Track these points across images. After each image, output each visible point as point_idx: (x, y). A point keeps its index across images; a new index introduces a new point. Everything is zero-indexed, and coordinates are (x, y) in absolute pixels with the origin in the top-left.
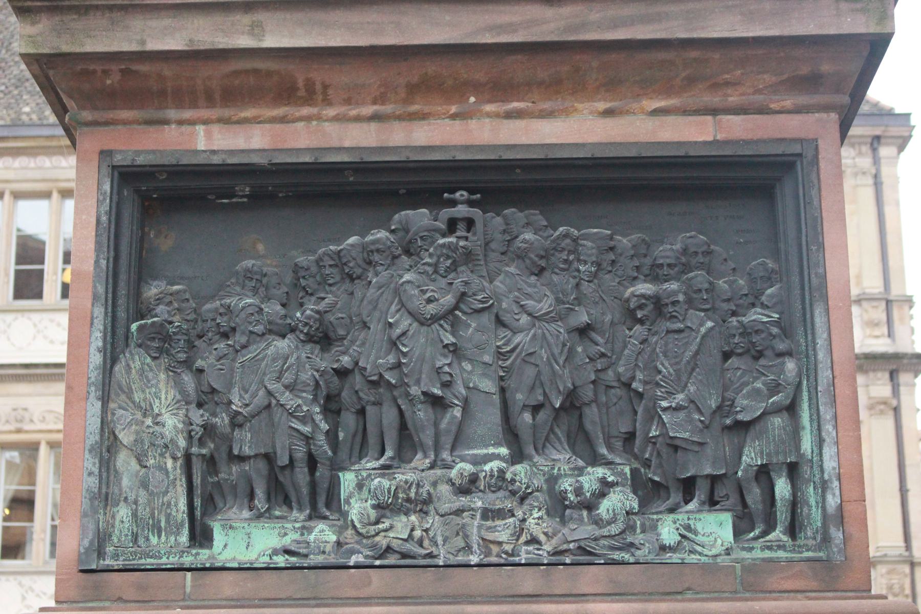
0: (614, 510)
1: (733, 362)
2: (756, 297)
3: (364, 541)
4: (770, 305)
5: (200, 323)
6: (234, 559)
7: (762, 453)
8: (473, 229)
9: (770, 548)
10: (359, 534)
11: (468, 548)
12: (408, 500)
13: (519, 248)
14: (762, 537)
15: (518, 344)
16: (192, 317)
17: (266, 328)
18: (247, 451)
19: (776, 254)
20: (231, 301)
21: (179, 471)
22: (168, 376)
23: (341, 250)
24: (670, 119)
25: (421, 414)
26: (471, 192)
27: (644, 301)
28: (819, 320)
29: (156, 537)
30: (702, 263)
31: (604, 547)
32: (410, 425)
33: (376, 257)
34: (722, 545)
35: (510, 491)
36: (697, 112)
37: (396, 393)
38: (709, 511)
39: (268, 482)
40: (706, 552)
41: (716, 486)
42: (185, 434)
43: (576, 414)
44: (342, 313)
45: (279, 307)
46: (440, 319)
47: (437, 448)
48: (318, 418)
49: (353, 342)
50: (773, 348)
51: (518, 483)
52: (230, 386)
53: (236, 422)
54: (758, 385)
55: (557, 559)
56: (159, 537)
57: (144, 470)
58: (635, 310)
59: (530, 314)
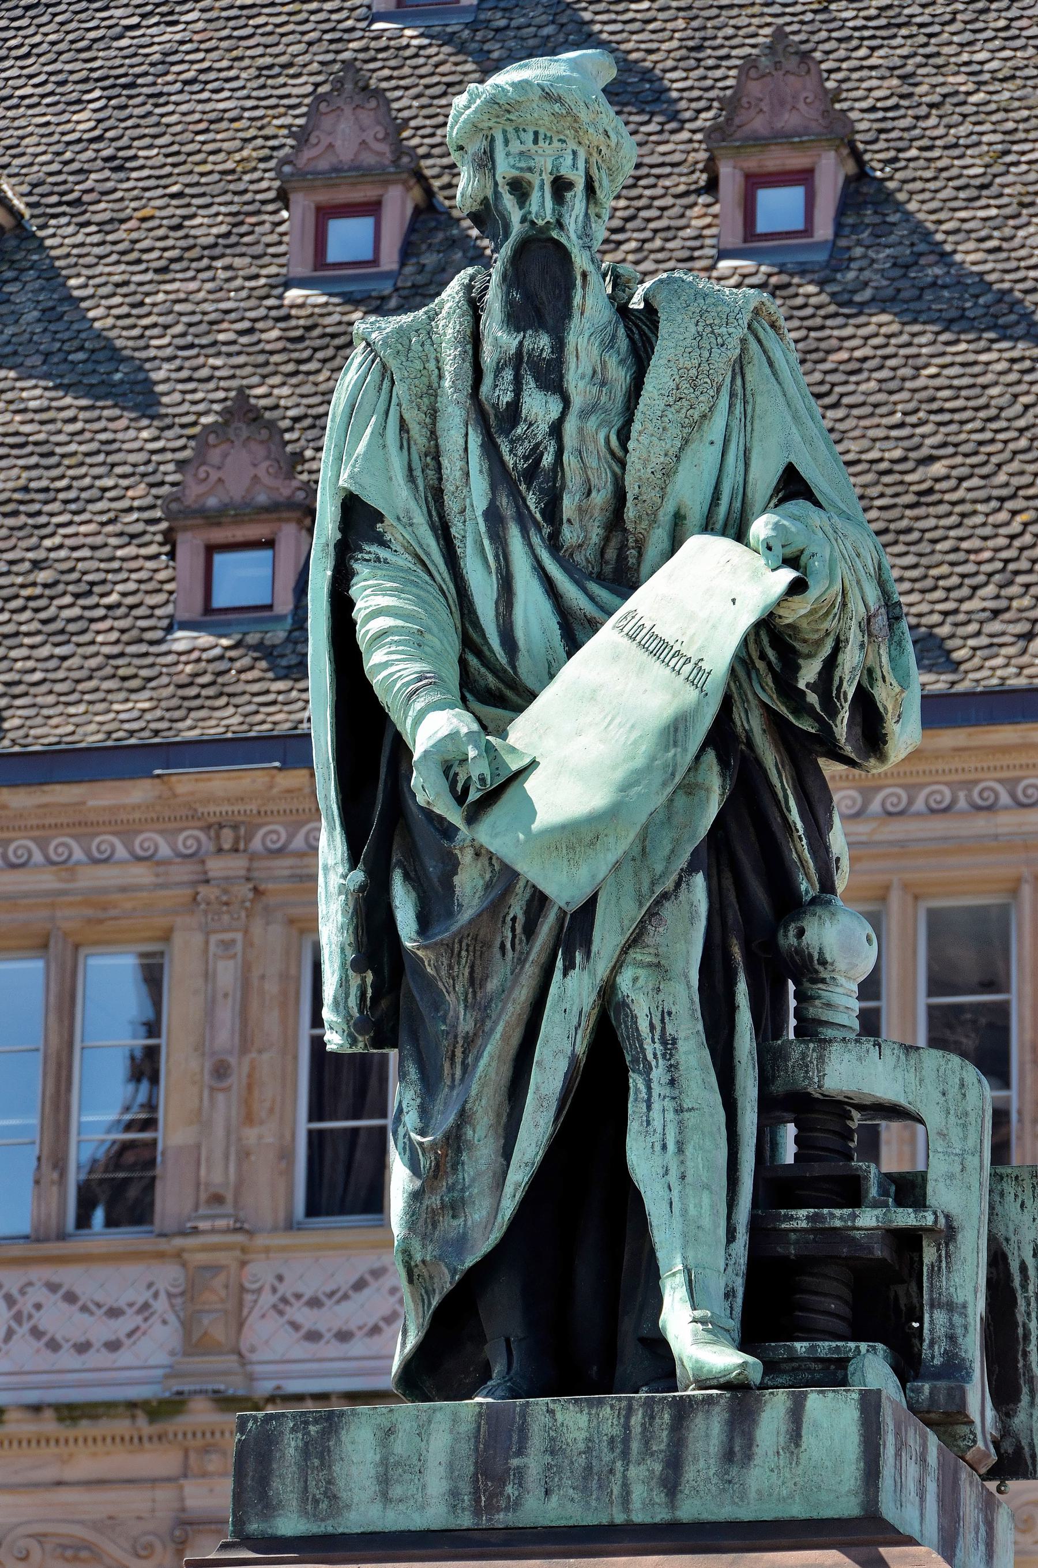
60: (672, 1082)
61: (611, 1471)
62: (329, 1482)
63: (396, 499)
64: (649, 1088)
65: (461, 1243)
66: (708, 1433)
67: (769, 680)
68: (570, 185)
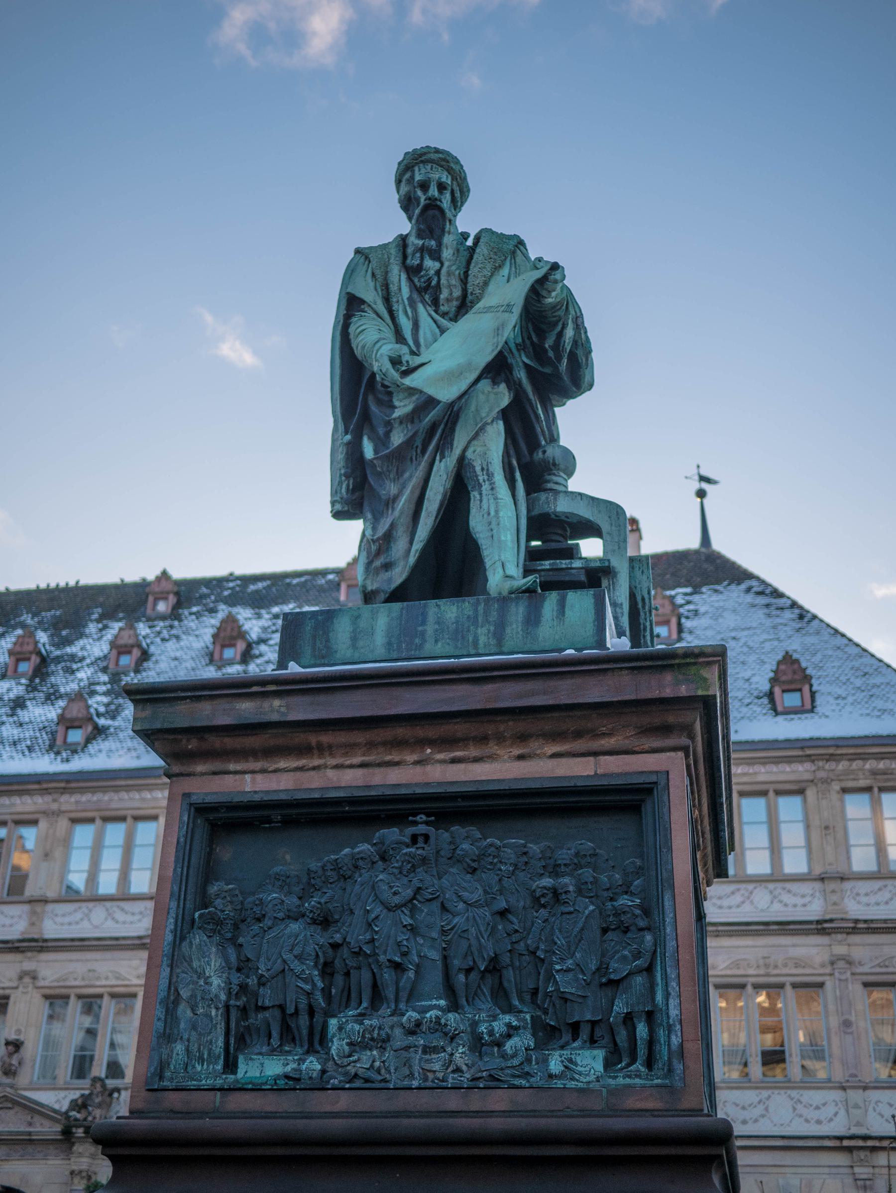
1: (610, 935)
7: (627, 1004)
9: (630, 1077)
10: (336, 1064)
11: (411, 1076)
12: (372, 1039)
18: (267, 1003)
19: (641, 856)
24: (564, 760)
25: (386, 976)
26: (428, 815)
28: (667, 904)
32: (379, 983)
33: (361, 863)
36: (583, 755)
37: (370, 960)
40: (582, 1079)
47: (397, 1001)
49: (343, 924)
50: (636, 925)
54: (626, 953)
56: (203, 1065)
58: (539, 898)
59: (465, 902)
60: (492, 489)
61: (469, 631)
62: (328, 641)
63: (368, 292)
64: (481, 494)
65: (390, 580)
66: (518, 612)
67: (531, 350)
68: (445, 188)
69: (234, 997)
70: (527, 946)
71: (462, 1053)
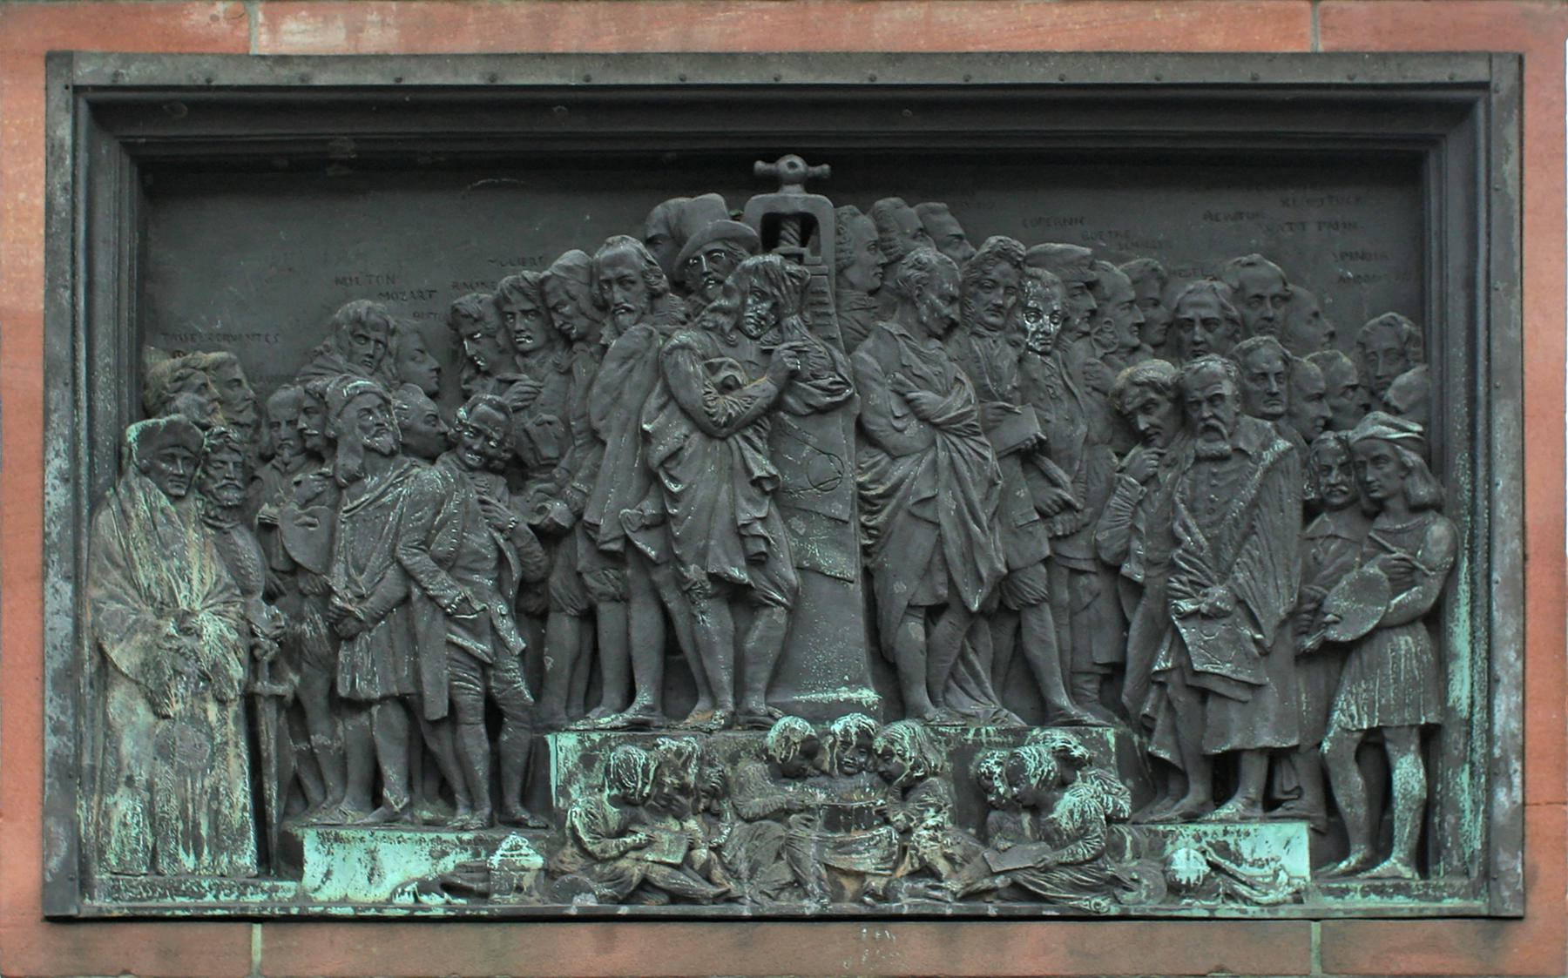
0: (1083, 813)
1: (1326, 522)
2: (1373, 394)
3: (597, 868)
4: (1402, 407)
5: (265, 430)
6: (344, 901)
8: (813, 238)
9: (1380, 891)
10: (585, 852)
11: (798, 884)
12: (683, 789)
13: (906, 279)
14: (1364, 870)
15: (902, 481)
16: (248, 416)
17: (396, 441)
20: (329, 384)
21: (231, 726)
22: (205, 536)
23: (547, 278)
25: (708, 621)
26: (811, 160)
27: (1153, 395)
29: (192, 857)
30: (1270, 320)
31: (1062, 885)
34: (1289, 884)
35: (881, 774)
37: (659, 576)
38: (1263, 820)
39: (409, 753)
41: (1277, 768)
42: (242, 654)
43: (1010, 625)
44: (547, 412)
45: (422, 399)
46: (746, 425)
47: (740, 687)
48: (506, 625)
49: (571, 473)
50: (1405, 495)
51: (896, 759)
52: (329, 556)
53: (341, 631)
54: (1373, 569)
55: (970, 914)
56: (198, 856)
57: (163, 723)
58: (1133, 413)
59: (924, 419)
69: (265, 671)
70: (1096, 547)
71: (936, 828)
